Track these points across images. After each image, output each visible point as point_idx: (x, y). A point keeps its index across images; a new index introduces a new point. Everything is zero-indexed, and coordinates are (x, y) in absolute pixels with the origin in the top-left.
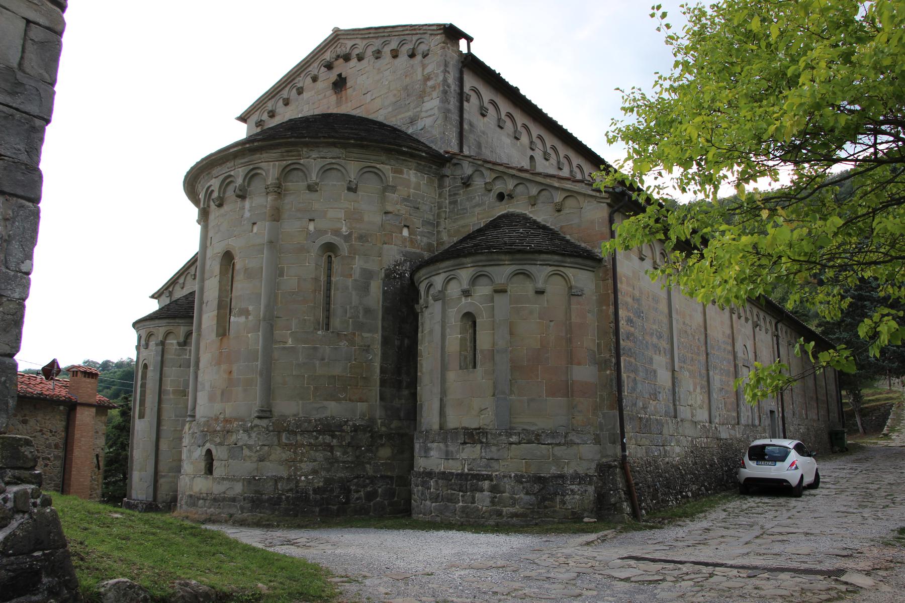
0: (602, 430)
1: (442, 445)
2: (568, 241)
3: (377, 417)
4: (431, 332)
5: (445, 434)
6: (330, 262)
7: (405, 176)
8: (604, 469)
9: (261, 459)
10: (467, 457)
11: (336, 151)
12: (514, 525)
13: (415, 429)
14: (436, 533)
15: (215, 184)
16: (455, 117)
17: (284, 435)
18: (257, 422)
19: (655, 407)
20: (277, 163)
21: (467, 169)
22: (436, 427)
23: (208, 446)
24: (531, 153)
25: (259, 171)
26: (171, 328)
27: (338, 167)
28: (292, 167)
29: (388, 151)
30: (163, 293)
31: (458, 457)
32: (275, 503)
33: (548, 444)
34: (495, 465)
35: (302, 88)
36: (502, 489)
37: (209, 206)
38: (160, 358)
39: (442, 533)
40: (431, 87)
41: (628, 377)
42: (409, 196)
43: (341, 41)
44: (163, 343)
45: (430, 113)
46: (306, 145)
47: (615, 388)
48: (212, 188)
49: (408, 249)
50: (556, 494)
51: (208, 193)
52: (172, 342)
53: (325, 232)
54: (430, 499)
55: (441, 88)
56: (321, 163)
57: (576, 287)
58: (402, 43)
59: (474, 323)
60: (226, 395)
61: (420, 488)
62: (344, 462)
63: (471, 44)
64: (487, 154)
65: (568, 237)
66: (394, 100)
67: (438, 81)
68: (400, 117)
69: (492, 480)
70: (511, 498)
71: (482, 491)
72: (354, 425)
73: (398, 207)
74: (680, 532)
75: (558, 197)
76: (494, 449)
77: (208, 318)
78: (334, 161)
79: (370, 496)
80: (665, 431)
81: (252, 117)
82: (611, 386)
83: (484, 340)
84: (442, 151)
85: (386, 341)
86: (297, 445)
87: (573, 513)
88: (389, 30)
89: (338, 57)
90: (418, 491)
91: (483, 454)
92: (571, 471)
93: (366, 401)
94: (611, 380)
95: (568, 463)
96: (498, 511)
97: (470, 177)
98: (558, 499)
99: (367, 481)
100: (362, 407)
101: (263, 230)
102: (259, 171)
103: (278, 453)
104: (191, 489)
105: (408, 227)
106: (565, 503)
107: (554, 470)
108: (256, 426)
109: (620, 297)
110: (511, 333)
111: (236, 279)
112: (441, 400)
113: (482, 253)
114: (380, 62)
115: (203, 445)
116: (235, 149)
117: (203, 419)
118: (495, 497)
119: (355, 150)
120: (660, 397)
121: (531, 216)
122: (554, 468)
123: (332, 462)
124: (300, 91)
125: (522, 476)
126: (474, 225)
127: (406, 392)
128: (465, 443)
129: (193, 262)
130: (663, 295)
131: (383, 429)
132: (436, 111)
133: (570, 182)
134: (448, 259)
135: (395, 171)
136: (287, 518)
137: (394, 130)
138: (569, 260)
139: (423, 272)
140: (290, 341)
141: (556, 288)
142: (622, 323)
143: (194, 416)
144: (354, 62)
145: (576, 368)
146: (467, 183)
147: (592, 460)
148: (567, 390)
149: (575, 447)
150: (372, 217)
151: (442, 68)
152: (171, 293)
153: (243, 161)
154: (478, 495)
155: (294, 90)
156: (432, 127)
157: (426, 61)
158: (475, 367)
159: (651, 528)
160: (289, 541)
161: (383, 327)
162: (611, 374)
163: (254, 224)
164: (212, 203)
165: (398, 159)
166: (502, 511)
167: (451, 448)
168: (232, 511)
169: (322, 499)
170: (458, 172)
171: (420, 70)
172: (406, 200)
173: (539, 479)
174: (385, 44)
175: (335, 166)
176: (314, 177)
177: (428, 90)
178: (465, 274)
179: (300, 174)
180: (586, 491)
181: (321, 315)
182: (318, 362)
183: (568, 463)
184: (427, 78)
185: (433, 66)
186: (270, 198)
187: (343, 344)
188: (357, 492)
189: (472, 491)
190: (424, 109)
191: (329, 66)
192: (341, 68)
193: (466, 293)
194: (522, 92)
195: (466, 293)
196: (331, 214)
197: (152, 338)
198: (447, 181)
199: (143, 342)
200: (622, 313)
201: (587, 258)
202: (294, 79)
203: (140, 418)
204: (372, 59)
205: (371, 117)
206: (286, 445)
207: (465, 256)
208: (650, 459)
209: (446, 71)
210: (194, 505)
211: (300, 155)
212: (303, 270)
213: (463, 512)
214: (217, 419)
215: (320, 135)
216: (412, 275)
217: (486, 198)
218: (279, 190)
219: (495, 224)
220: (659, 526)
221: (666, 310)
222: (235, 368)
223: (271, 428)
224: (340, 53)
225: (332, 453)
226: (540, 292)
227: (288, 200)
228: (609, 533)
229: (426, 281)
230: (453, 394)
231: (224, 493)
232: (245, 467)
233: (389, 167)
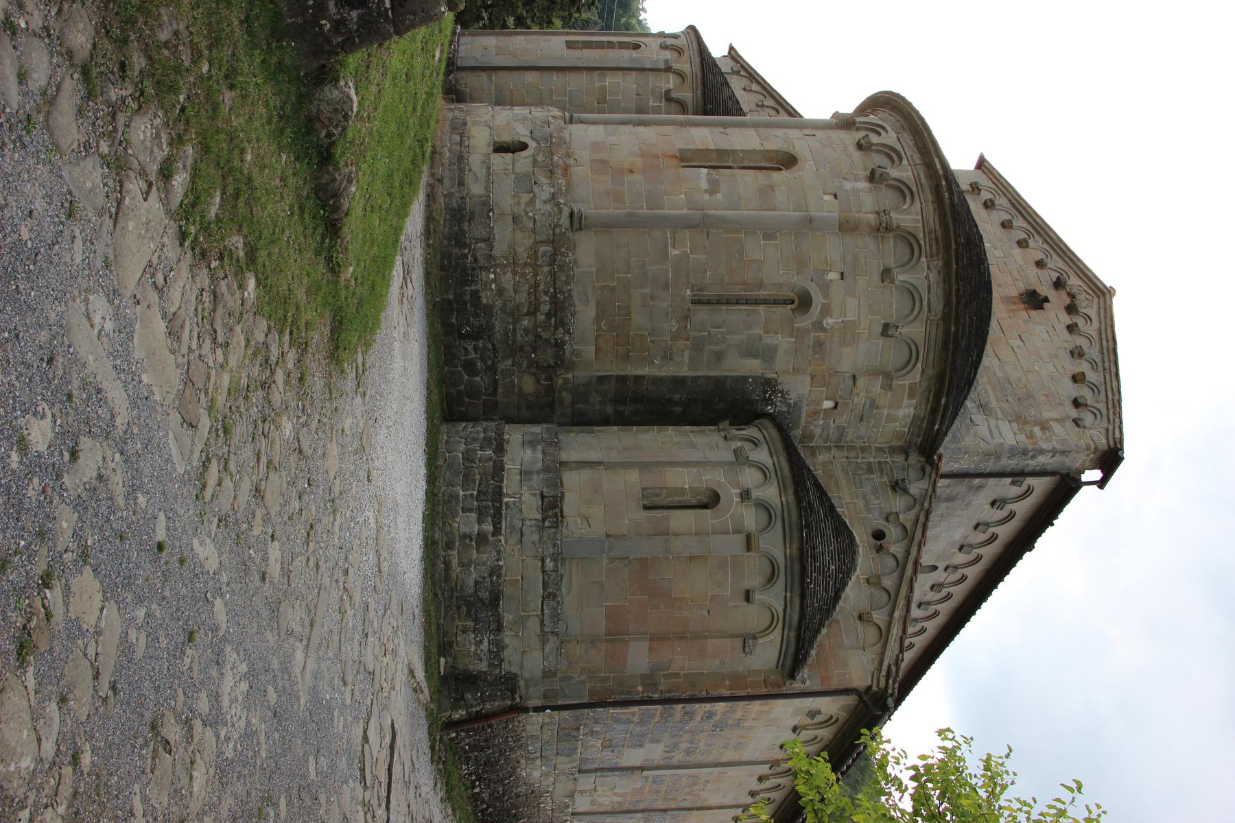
0: (562, 679)
1: (539, 465)
2: (818, 631)
3: (577, 373)
4: (692, 446)
5: (554, 470)
6: (785, 302)
7: (906, 401)
8: (510, 683)
9: (516, 219)
10: (523, 500)
11: (938, 306)
12: (434, 565)
13: (560, 425)
14: (422, 463)
15: (889, 138)
16: (990, 466)
17: (548, 248)
18: (566, 211)
19: (594, 746)
22: (564, 456)
24: (941, 567)
25: (908, 200)
26: (690, 80)
27: (916, 310)
29: (940, 378)
30: (738, 62)
31: (524, 488)
32: (459, 239)
33: (543, 610)
34: (515, 538)
35: (1027, 246)
36: (482, 549)
37: (858, 129)
38: (648, 66)
39: (423, 471)
41: (634, 714)
42: (878, 407)
43: (1096, 300)
44: (668, 69)
46: (947, 265)
47: (618, 698)
48: (883, 133)
50: (476, 621)
51: (876, 129)
52: (671, 82)
53: (826, 295)
54: (467, 451)
55: (1030, 447)
56: (922, 286)
57: (755, 645)
58: (1094, 388)
59: (704, 506)
60: (601, 165)
61: (482, 435)
62: (514, 330)
64: (939, 509)
65: (824, 631)
66: (1012, 379)
68: (989, 388)
69: (493, 535)
70: (470, 562)
71: (480, 522)
72: (564, 343)
73: (863, 394)
74: (426, 790)
75: (879, 617)
76: (536, 537)
78: (925, 303)
79: (470, 367)
80: (561, 759)
81: (984, 177)
82: (621, 693)
83: (681, 520)
84: (941, 450)
85: (678, 382)
86: (536, 268)
87: (451, 644)
88: (1113, 369)
89: (1072, 296)
90: (478, 432)
91: (528, 523)
92: (507, 640)
94: (629, 693)
95: (517, 636)
96: (453, 543)
97: (905, 491)
98: (470, 624)
99: (490, 362)
100: (589, 351)
101: (826, 208)
102: (908, 200)
103: (524, 243)
104: (475, 123)
105: (836, 407)
106: (464, 632)
107: (508, 618)
108: (561, 210)
109: (742, 703)
110: (691, 558)
112: (600, 463)
113: (800, 516)
114: (1067, 357)
116: (938, 166)
117: (567, 136)
118: (471, 540)
119: (940, 332)
120: (607, 753)
121: (853, 578)
123: (515, 315)
124: (1022, 244)
125: (499, 576)
126: (839, 498)
127: (609, 410)
128: (543, 497)
130: (746, 756)
131: (560, 382)
132: (998, 440)
133: (900, 633)
134: (792, 469)
135: (912, 388)
136: (438, 257)
137: (970, 382)
138: (793, 634)
139: (774, 433)
140: (676, 252)
141: (753, 617)
142: (708, 706)
143: (571, 122)
144: (1066, 319)
145: (645, 646)
146: (897, 487)
147: (521, 668)
148: (616, 635)
149: (539, 645)
150: (848, 359)
151: (1059, 447)
152: (738, 73)
153: (922, 176)
154: (473, 516)
155: (1025, 236)
156: (976, 435)
157: (1069, 424)
158: (646, 508)
159: (432, 748)
160: (409, 272)
161: (698, 377)
162: (638, 692)
163: (835, 196)
164: (863, 134)
165: (930, 391)
166: (452, 549)
167: (535, 477)
168: (446, 181)
169: (465, 303)
170: (913, 474)
171: (1055, 415)
172: (873, 404)
173: (496, 598)
174: (1093, 364)
175: (917, 305)
176: (901, 277)
177: (1028, 428)
178: (770, 493)
179: (906, 258)
180: (481, 660)
181: (713, 292)
182: (648, 290)
183: (517, 636)
184: (1044, 427)
185: (1063, 433)
186: (871, 217)
187: (674, 325)
188: (476, 349)
189: (479, 508)
190: (1000, 423)
191: (1058, 284)
192: (1058, 301)
193: (745, 495)
194: (1027, 555)
195: (745, 495)
196: (851, 302)
197: (676, 54)
198: (900, 459)
199: (670, 41)
200: (720, 706)
201: (796, 657)
203: (567, 42)
204: (1070, 346)
205: (988, 346)
206: (536, 252)
207: (796, 493)
208: (523, 741)
209: (1054, 452)
210: (454, 128)
211: (932, 256)
212: (773, 267)
213: (451, 496)
214: (568, 155)
215: (961, 283)
216: (771, 417)
217: (877, 514)
218: (883, 229)
219: (842, 529)
220: (435, 757)
221: (724, 759)
222: (637, 177)
224: (1078, 299)
225: (526, 314)
226: (748, 596)
227: (870, 242)
228: (426, 695)
229: (760, 437)
230: (608, 476)
231: (470, 170)
232: (506, 198)
233: (918, 380)
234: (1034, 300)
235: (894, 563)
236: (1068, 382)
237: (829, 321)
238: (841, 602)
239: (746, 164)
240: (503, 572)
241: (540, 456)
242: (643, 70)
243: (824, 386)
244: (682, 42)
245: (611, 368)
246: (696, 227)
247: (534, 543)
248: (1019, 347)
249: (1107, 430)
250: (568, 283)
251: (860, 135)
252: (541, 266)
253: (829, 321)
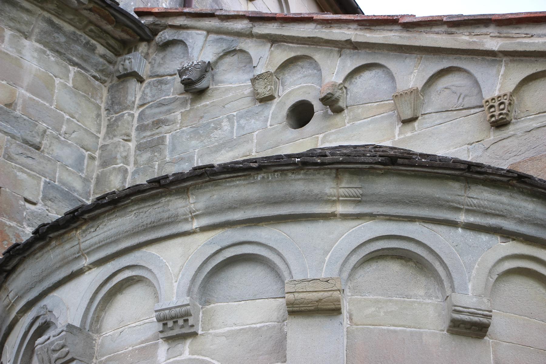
21: (201, 47)
97: (207, 68)
146: (195, 87)
170: (173, 63)
217: (254, 124)
235: (367, 75)
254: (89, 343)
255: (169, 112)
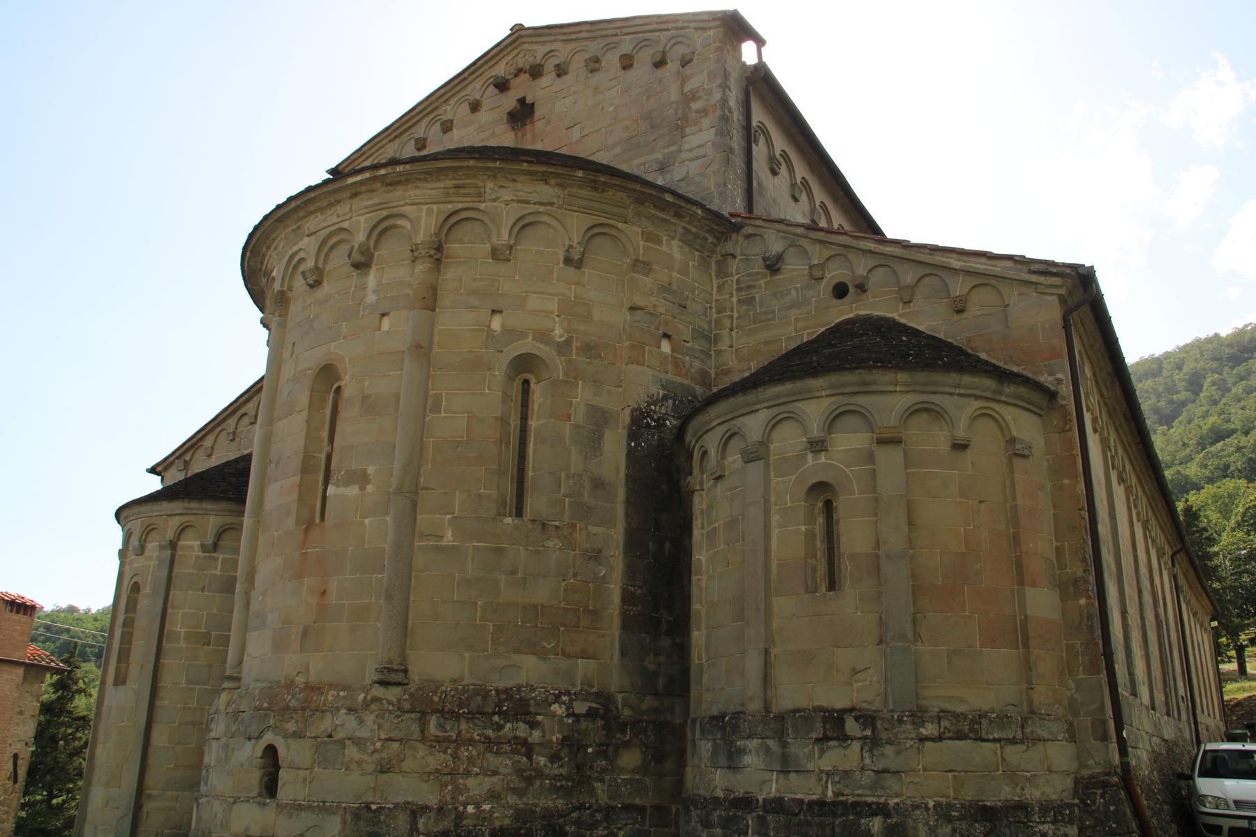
0: (1075, 713)
7: (664, 248)
9: (384, 768)
15: (307, 246)
16: (739, 162)
17: (433, 720)
18: (379, 691)
20: (435, 207)
22: (755, 706)
23: (269, 738)
28: (463, 215)
31: (810, 766)
35: (451, 122)
38: (166, 573)
40: (697, 112)
43: (526, 46)
45: (696, 153)
49: (670, 377)
52: (191, 545)
53: (523, 335)
55: (719, 113)
57: (1022, 441)
58: (642, 45)
63: (763, 49)
65: (983, 356)
67: (713, 102)
73: (653, 299)
77: (274, 492)
82: (1091, 628)
83: (855, 535)
84: (725, 213)
85: (633, 543)
86: (460, 741)
89: (520, 71)
93: (594, 658)
97: (780, 257)
99: (599, 816)
100: (583, 668)
101: (398, 328)
105: (666, 336)
108: (375, 699)
110: (911, 523)
111: (344, 414)
112: (767, 652)
115: (260, 737)
117: (259, 685)
122: (1008, 789)
123: (529, 777)
124: (447, 127)
125: (950, 806)
126: (788, 340)
128: (825, 738)
129: (255, 390)
131: (627, 712)
132: (709, 149)
135: (651, 238)
141: (986, 441)
144: (547, 80)
146: (773, 265)
147: (1067, 773)
148: (1021, 634)
149: (1040, 745)
155: (438, 125)
157: (688, 71)
162: (1089, 605)
163: (383, 315)
164: (299, 277)
170: (755, 250)
172: (666, 289)
178: (815, 411)
184: (693, 97)
186: (419, 268)
190: (686, 147)
192: (522, 88)
193: (817, 446)
196: (534, 303)
197: (153, 535)
198: (733, 265)
202: (436, 108)
206: (438, 740)
209: (725, 87)
214: (290, 685)
218: (437, 253)
222: (333, 585)
223: (407, 706)
224: (523, 61)
225: (530, 758)
226: (960, 447)
234: (522, 114)
235: (881, 270)
236: (631, 74)
237: (558, 333)
238: (941, 336)
239: (325, 434)
240: (944, 800)
241: (755, 743)
242: (169, 579)
243: (643, 349)
244: (137, 526)
245: (610, 634)
246: (415, 504)
247: (899, 753)
248: (582, 129)
249: (696, 29)
250: (486, 695)
251: (299, 283)
252: (459, 732)
253: (558, 333)
254: (767, 448)
255: (756, 280)
